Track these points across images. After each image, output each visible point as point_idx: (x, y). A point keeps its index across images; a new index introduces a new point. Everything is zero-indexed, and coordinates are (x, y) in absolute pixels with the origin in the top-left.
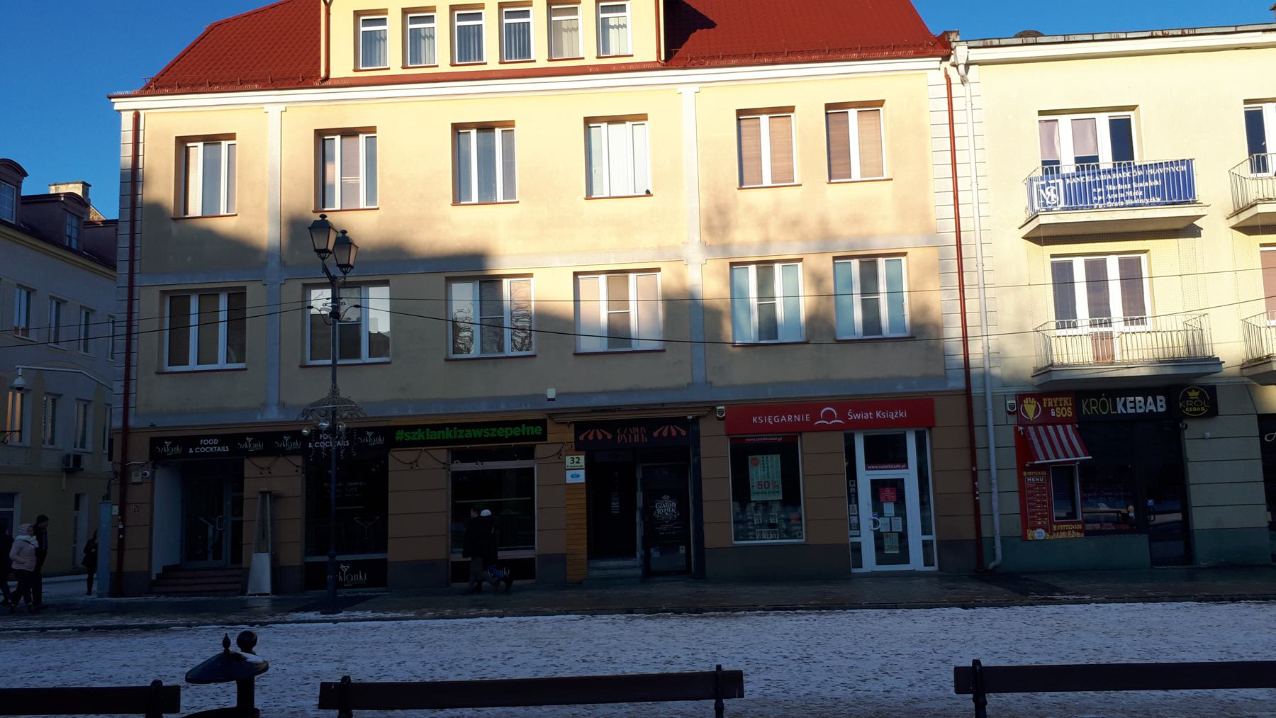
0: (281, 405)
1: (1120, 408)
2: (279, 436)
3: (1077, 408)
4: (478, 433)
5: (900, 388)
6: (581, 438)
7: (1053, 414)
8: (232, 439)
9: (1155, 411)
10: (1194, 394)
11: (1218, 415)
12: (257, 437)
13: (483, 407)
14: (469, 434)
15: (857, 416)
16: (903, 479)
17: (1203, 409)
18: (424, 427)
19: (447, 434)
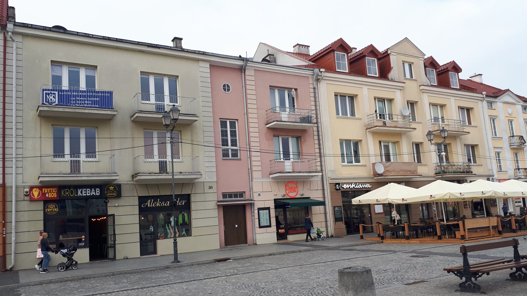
1: (79, 194)
3: (59, 193)
7: (47, 196)
9: (95, 195)
11: (121, 197)
17: (115, 194)
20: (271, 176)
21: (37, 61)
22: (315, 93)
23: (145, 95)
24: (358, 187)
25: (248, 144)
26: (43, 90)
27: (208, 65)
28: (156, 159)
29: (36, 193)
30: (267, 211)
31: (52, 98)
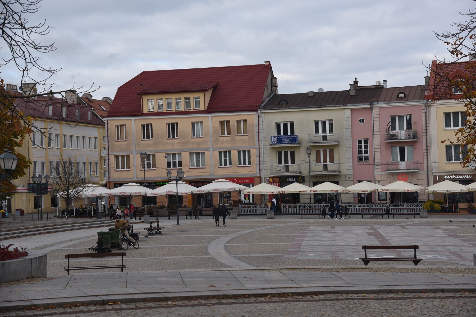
0: (137, 177)
1: (287, 180)
3: (279, 180)
5: (248, 176)
10: (300, 178)
15: (240, 181)
18: (162, 182)
20: (387, 172)
21: (270, 123)
22: (426, 115)
23: (317, 131)
24: (459, 177)
26: (272, 136)
27: (350, 111)
28: (322, 163)
29: (271, 180)
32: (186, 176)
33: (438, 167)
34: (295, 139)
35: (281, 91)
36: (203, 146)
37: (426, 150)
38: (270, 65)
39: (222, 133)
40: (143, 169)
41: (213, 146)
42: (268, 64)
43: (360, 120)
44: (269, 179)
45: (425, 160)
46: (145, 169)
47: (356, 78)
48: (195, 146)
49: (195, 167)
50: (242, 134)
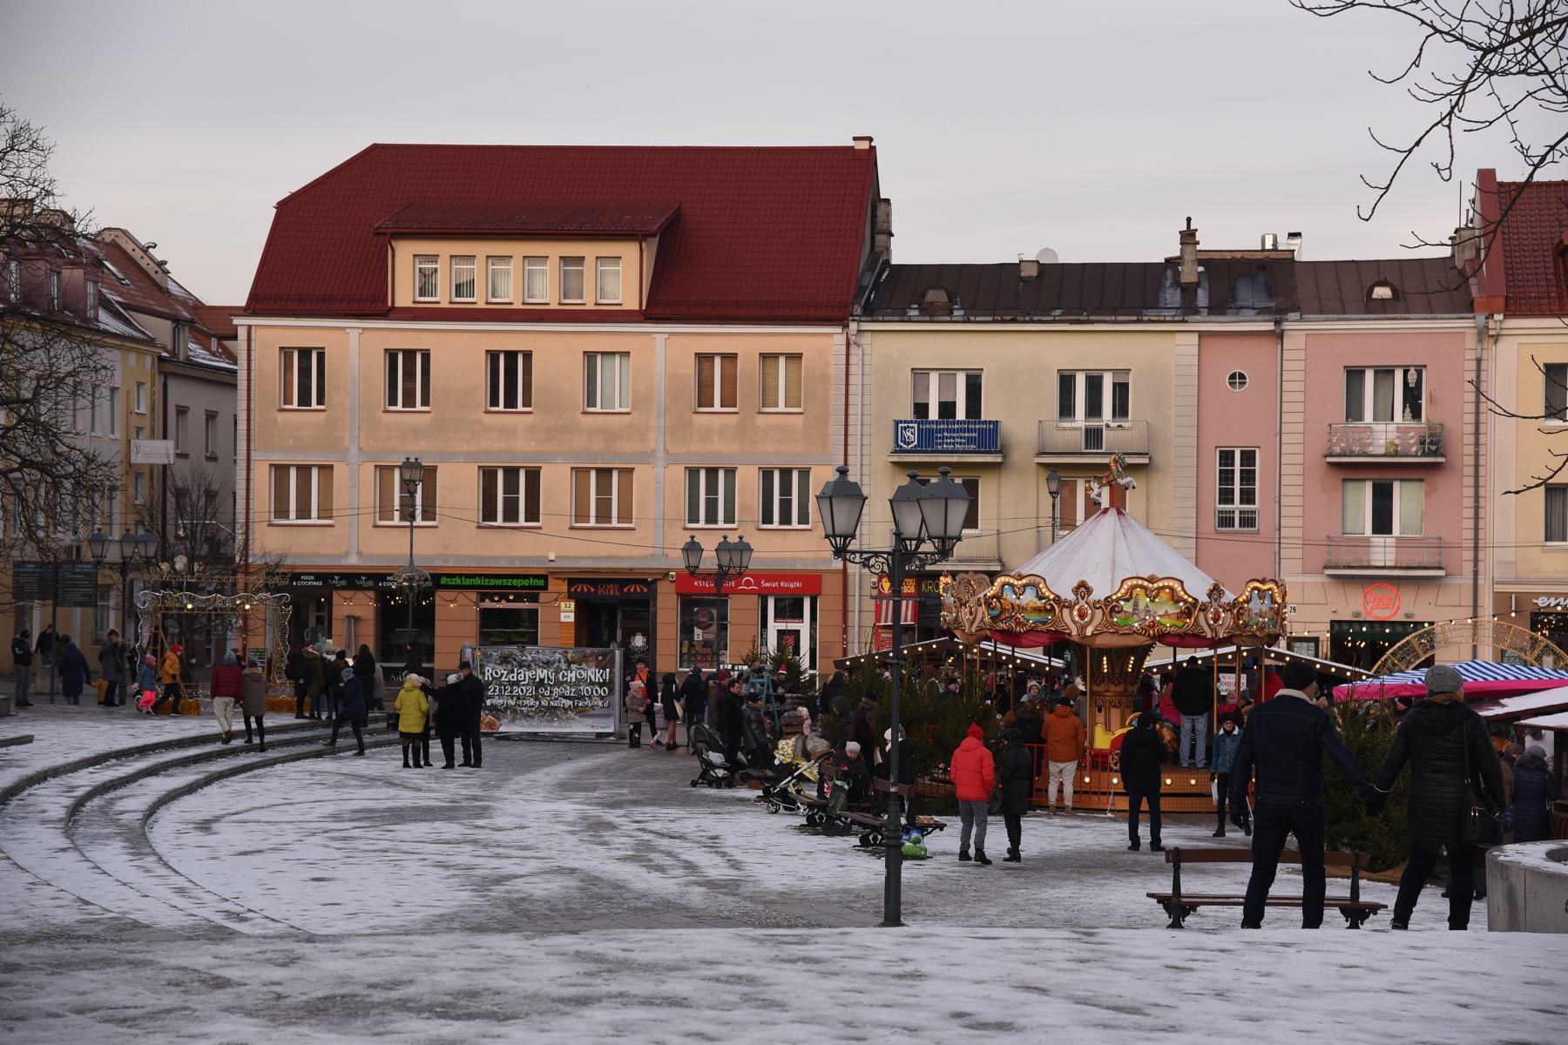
0: (359, 554)
2: (358, 576)
3: (918, 586)
4: (499, 582)
5: (799, 566)
6: (572, 590)
8: (324, 577)
12: (343, 576)
13: (503, 564)
14: (493, 582)
15: (768, 585)
16: (799, 631)
18: (461, 576)
19: (477, 581)
21: (891, 372)
23: (1066, 409)
25: (1277, 500)
26: (897, 423)
27: (1195, 337)
30: (1312, 644)
31: (909, 434)
32: (556, 557)
33: (1515, 563)
34: (989, 437)
35: (906, 249)
36: (627, 447)
37: (1473, 500)
38: (873, 149)
39: (704, 399)
40: (408, 524)
41: (669, 447)
42: (864, 145)
43: (1233, 376)
44: (880, 580)
45: (1470, 534)
46: (414, 524)
47: (1189, 220)
48: (597, 445)
49: (592, 523)
50: (781, 408)
